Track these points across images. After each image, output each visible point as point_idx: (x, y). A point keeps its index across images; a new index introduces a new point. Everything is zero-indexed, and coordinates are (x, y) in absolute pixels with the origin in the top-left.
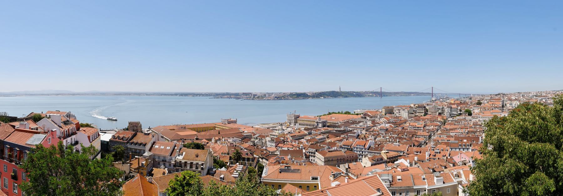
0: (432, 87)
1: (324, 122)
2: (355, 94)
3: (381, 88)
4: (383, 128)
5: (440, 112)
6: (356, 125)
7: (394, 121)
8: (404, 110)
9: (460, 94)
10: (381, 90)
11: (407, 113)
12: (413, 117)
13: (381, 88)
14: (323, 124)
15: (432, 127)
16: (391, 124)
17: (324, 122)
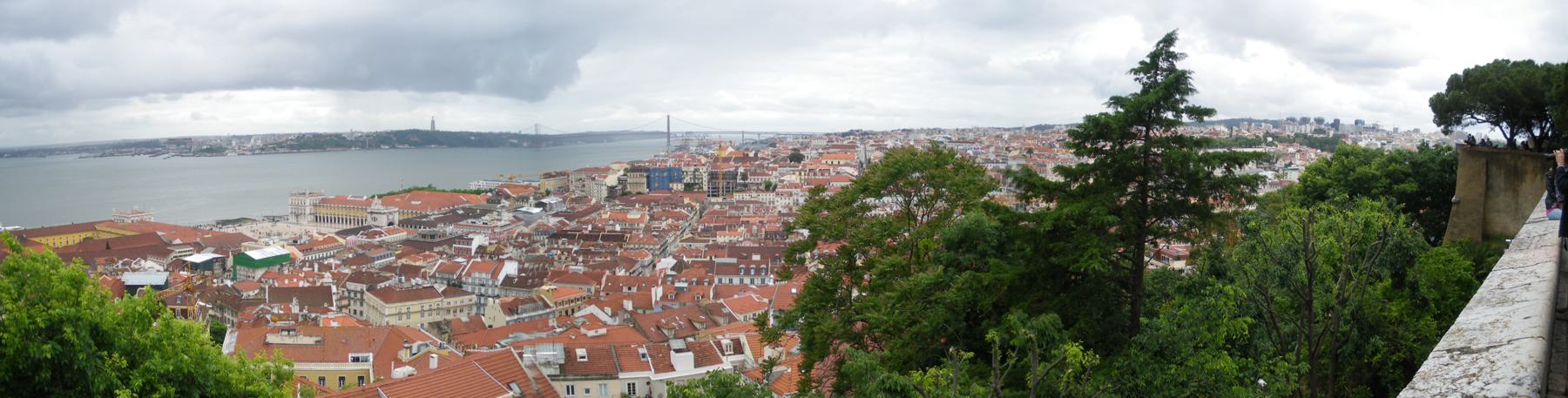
0: (668, 117)
8: (594, 179)
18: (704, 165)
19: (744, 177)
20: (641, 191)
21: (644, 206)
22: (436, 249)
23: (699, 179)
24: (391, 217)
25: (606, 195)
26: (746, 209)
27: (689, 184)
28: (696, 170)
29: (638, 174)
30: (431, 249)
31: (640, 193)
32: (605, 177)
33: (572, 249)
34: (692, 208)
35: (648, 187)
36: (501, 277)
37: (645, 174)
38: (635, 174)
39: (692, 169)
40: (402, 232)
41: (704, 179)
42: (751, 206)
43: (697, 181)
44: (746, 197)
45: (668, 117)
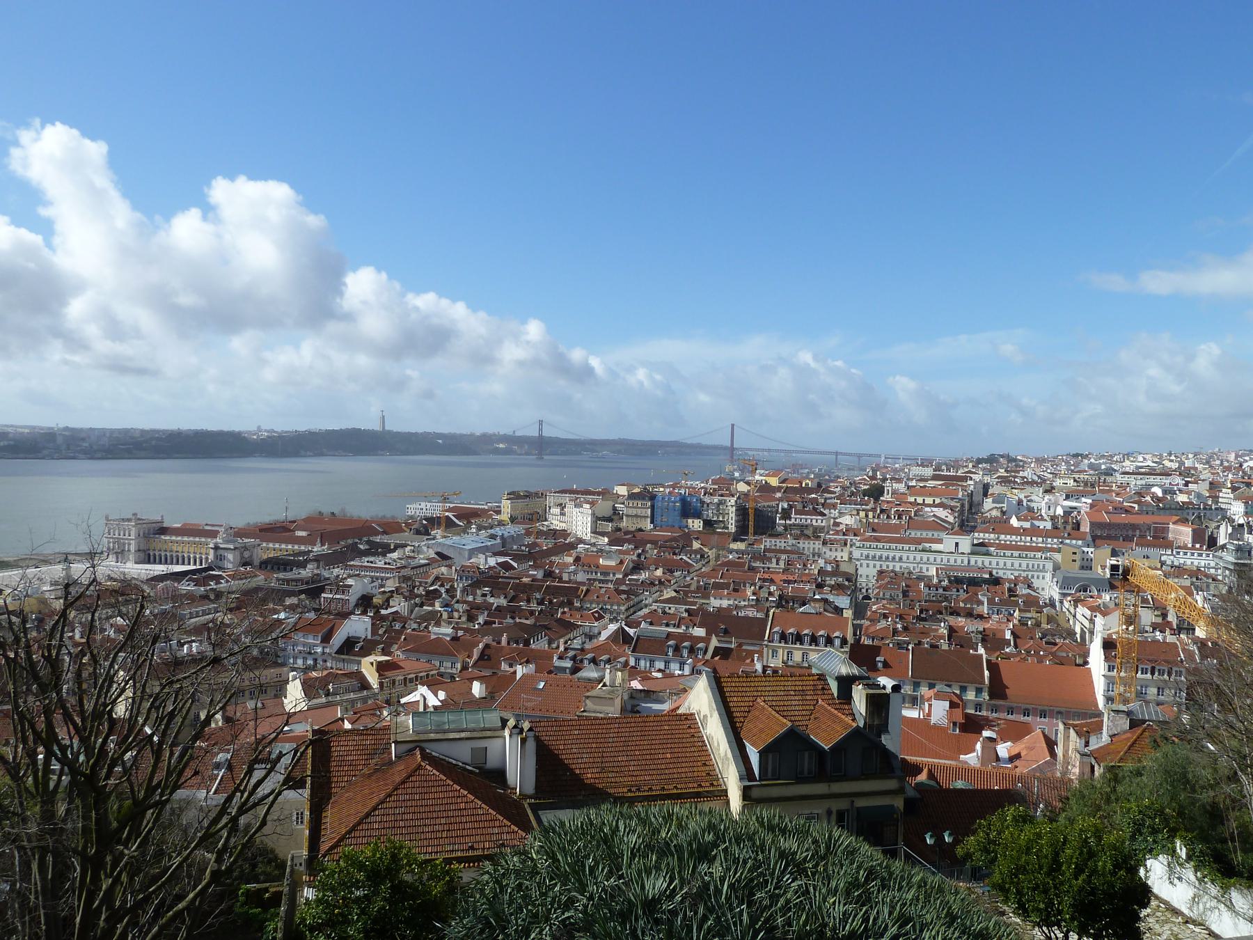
0: (733, 425)
2: (440, 441)
3: (541, 423)
6: (372, 559)
7: (523, 548)
8: (578, 506)
9: (837, 454)
10: (541, 430)
11: (589, 519)
13: (541, 423)
14: (242, 557)
15: (659, 572)
16: (507, 559)
18: (733, 496)
19: (786, 514)
21: (636, 548)
24: (246, 554)
26: (774, 560)
28: (720, 503)
29: (640, 503)
34: (702, 556)
35: (652, 522)
36: (338, 639)
40: (256, 576)
42: (783, 557)
44: (780, 543)
45: (733, 425)
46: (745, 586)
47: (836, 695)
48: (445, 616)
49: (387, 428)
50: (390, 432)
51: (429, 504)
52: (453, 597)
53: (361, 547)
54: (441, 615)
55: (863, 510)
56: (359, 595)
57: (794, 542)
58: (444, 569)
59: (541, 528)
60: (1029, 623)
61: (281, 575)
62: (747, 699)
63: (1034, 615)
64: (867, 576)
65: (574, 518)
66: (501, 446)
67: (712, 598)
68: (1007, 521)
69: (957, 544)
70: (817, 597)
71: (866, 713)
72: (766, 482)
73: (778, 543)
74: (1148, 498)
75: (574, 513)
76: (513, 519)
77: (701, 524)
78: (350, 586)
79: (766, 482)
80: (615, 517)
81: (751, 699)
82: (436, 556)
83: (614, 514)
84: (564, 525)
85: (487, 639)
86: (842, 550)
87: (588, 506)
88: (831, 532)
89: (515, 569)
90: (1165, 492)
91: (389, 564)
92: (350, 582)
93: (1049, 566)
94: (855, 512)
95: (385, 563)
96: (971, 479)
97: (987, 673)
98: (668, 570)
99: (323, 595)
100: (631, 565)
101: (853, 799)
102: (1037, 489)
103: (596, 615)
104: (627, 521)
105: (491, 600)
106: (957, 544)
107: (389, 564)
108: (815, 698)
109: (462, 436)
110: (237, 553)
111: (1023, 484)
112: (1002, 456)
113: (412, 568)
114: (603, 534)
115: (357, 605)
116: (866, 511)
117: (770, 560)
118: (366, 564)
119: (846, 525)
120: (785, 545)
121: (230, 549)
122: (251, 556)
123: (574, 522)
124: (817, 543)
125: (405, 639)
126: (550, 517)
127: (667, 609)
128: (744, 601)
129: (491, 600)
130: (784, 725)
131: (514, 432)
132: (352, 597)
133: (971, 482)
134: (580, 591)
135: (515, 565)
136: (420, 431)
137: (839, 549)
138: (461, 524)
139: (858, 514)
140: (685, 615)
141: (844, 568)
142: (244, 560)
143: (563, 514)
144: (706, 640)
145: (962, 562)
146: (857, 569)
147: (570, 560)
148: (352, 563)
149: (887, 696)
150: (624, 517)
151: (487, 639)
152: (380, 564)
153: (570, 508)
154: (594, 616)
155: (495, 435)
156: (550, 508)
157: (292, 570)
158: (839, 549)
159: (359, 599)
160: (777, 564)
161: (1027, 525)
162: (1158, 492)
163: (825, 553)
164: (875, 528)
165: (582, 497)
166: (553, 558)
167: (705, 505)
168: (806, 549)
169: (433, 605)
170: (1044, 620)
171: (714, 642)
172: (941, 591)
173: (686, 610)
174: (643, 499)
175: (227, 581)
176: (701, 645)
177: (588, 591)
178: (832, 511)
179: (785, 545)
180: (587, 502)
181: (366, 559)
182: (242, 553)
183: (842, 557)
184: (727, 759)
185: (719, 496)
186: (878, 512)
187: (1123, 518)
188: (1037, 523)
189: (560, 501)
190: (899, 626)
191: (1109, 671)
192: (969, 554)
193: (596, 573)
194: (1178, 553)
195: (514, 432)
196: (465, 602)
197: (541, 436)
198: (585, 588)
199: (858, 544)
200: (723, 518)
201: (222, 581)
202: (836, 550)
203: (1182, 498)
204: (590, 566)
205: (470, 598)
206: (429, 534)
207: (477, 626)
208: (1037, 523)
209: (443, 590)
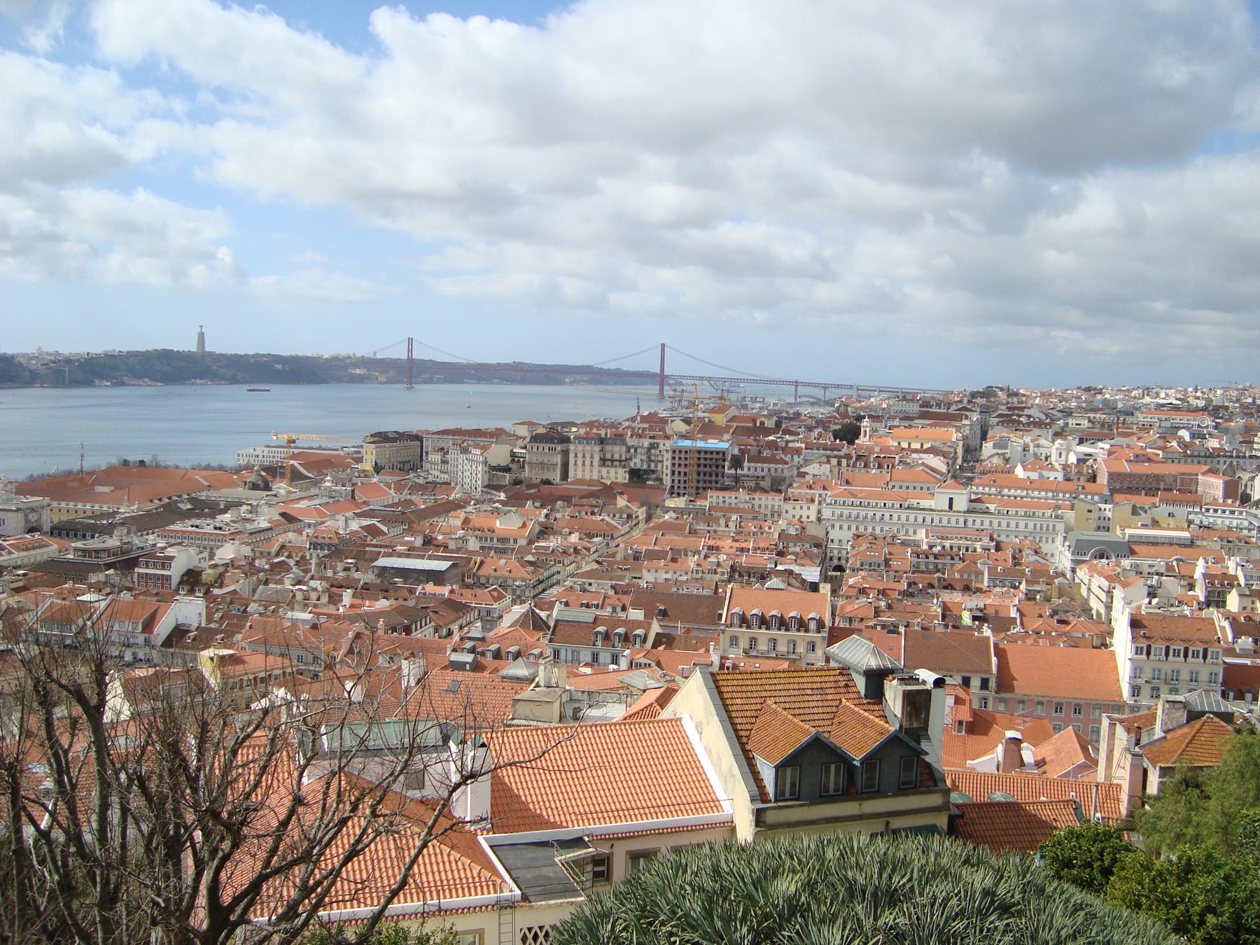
0: (663, 346)
1: (33, 510)
2: (279, 366)
3: (410, 341)
4: (327, 541)
5: (638, 466)
6: (198, 522)
8: (465, 451)
10: (410, 350)
11: (480, 468)
12: (505, 486)
13: (410, 341)
14: (27, 521)
15: (574, 538)
16: (374, 521)
17: (33, 510)
19: (737, 462)
20: (551, 478)
22: (93, 578)
23: (657, 463)
24: (33, 517)
25: (486, 483)
26: (722, 522)
27: (639, 470)
28: (652, 446)
30: (81, 578)
31: (547, 482)
32: (485, 449)
33: (360, 580)
34: (629, 517)
36: (163, 628)
37: (559, 448)
38: (541, 446)
39: (646, 443)
41: (666, 463)
42: (734, 517)
43: (653, 467)
44: (729, 498)
45: (663, 346)
46: (686, 555)
47: (863, 693)
48: (299, 596)
49: (209, 347)
50: (211, 354)
51: (266, 450)
52: (306, 571)
53: (182, 506)
54: (294, 596)
55: (835, 457)
56: (184, 570)
57: (747, 498)
58: (291, 535)
59: (417, 481)
60: (1038, 597)
61: (79, 544)
62: (752, 701)
63: (1044, 588)
64: (840, 541)
65: (460, 467)
66: (358, 371)
67: (645, 572)
68: (1011, 471)
69: (951, 499)
70: (779, 568)
71: (903, 714)
72: (710, 421)
73: (728, 500)
74: (1174, 444)
75: (460, 461)
76: (378, 469)
77: (627, 476)
78: (172, 558)
79: (710, 421)
80: (514, 467)
81: (758, 700)
82: (280, 518)
83: (513, 461)
84: (446, 476)
85: (359, 626)
86: (809, 508)
87: (478, 452)
88: (795, 485)
89: (383, 533)
90: (1193, 436)
91: (220, 529)
92: (171, 551)
93: (1060, 527)
94: (824, 459)
95: (215, 528)
96: (967, 418)
97: (994, 659)
98: (585, 534)
99: (136, 570)
100: (537, 529)
101: (889, 819)
102: (1045, 431)
103: (495, 594)
104: (531, 471)
105: (357, 575)
106: (951, 499)
107: (220, 529)
108: (838, 697)
109: (306, 358)
110: (21, 516)
111: (1028, 424)
112: (1001, 389)
113: (251, 534)
114: (498, 488)
115: (180, 583)
116: (839, 457)
117: (717, 520)
118: (190, 528)
119: (814, 475)
120: (736, 501)
121: (11, 510)
122: (39, 519)
123: (460, 473)
124: (777, 498)
125: (251, 627)
126: (426, 466)
127: (587, 586)
128: (686, 573)
129: (357, 575)
130: (805, 732)
131: (375, 353)
132: (175, 572)
133: (967, 422)
134: (472, 562)
135: (385, 529)
136: (251, 352)
137: (805, 507)
138: (310, 475)
139: (828, 462)
140: (611, 592)
141: (813, 530)
142: (30, 525)
143: (445, 462)
144: (646, 625)
145: (957, 522)
146: (827, 533)
147: (458, 522)
148: (172, 527)
149: (928, 693)
150: (526, 466)
151: (359, 626)
152: (210, 529)
153: (454, 456)
154: (492, 596)
155: (349, 357)
156: (427, 453)
157: (93, 537)
158: (805, 507)
159: (183, 575)
160: (727, 526)
161: (1034, 476)
162: (1185, 434)
163: (787, 512)
164: (850, 480)
165: (470, 441)
166: (435, 519)
167: (632, 451)
168: (763, 507)
169: (281, 582)
170: (1055, 593)
171: (656, 628)
172: (931, 559)
173: (613, 587)
174: (552, 442)
175: (10, 553)
176: (640, 632)
177: (482, 563)
178: (796, 457)
179: (736, 501)
180: (477, 446)
181: (190, 523)
182: (26, 516)
183: (808, 517)
184: (733, 776)
185: (652, 438)
186: (854, 459)
187: (1145, 468)
188: (1046, 474)
189: (443, 445)
190: (883, 604)
191: (1137, 654)
192: (965, 512)
193: (492, 539)
194: (1208, 510)
195: (375, 353)
196: (321, 578)
197: (411, 360)
198: (479, 559)
199: (828, 500)
200: (656, 466)
201: (3, 553)
202: (801, 508)
203: (1213, 443)
204: (483, 530)
205: (329, 573)
206: (270, 489)
207: (341, 610)
208: (1046, 474)
209: (292, 562)
